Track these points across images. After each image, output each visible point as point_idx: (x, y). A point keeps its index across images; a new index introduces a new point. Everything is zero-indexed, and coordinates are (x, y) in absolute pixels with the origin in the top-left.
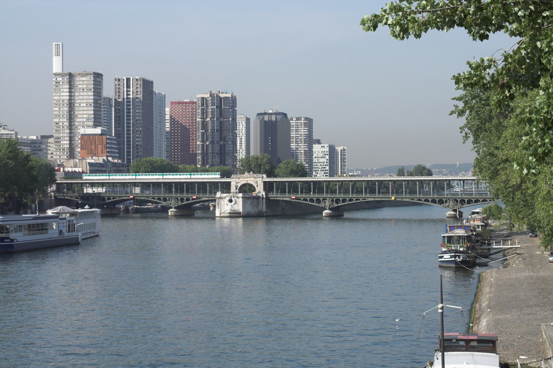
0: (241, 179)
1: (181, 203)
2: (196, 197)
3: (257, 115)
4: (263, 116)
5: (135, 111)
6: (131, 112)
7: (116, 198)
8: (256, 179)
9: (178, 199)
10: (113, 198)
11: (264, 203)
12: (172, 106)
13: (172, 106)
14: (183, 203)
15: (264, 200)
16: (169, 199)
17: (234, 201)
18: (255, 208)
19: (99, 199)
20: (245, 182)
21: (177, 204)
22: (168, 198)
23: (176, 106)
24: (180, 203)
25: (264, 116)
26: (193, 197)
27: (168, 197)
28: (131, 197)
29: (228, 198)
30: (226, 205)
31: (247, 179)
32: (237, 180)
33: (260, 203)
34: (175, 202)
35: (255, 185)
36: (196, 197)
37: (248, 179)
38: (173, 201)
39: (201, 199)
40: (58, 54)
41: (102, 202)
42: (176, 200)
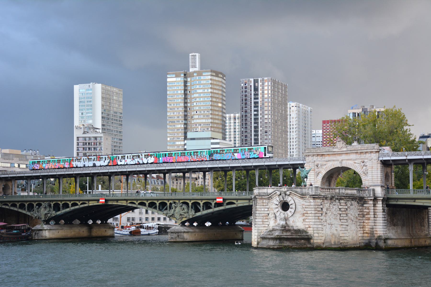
0: (327, 158)
1: (193, 212)
2: (222, 200)
3: (419, 138)
4: (426, 139)
5: (263, 116)
6: (259, 119)
7: (77, 205)
8: (363, 156)
9: (187, 204)
10: (73, 205)
11: (380, 214)
12: (324, 125)
13: (324, 125)
14: (198, 214)
15: (380, 205)
16: (171, 204)
17: (293, 206)
18: (353, 227)
19: (50, 206)
20: (337, 164)
21: (186, 215)
22: (168, 205)
23: (328, 125)
24: (192, 214)
25: (427, 139)
26: (218, 200)
27: (168, 200)
28: (100, 201)
29: (276, 200)
30: (271, 216)
31: (340, 158)
32: (319, 160)
33: (368, 213)
34: (182, 212)
35: (359, 170)
36: (222, 200)
37: (344, 157)
38: (178, 209)
39: (234, 203)
40: (194, 66)
41: (54, 212)
42: (184, 206)
